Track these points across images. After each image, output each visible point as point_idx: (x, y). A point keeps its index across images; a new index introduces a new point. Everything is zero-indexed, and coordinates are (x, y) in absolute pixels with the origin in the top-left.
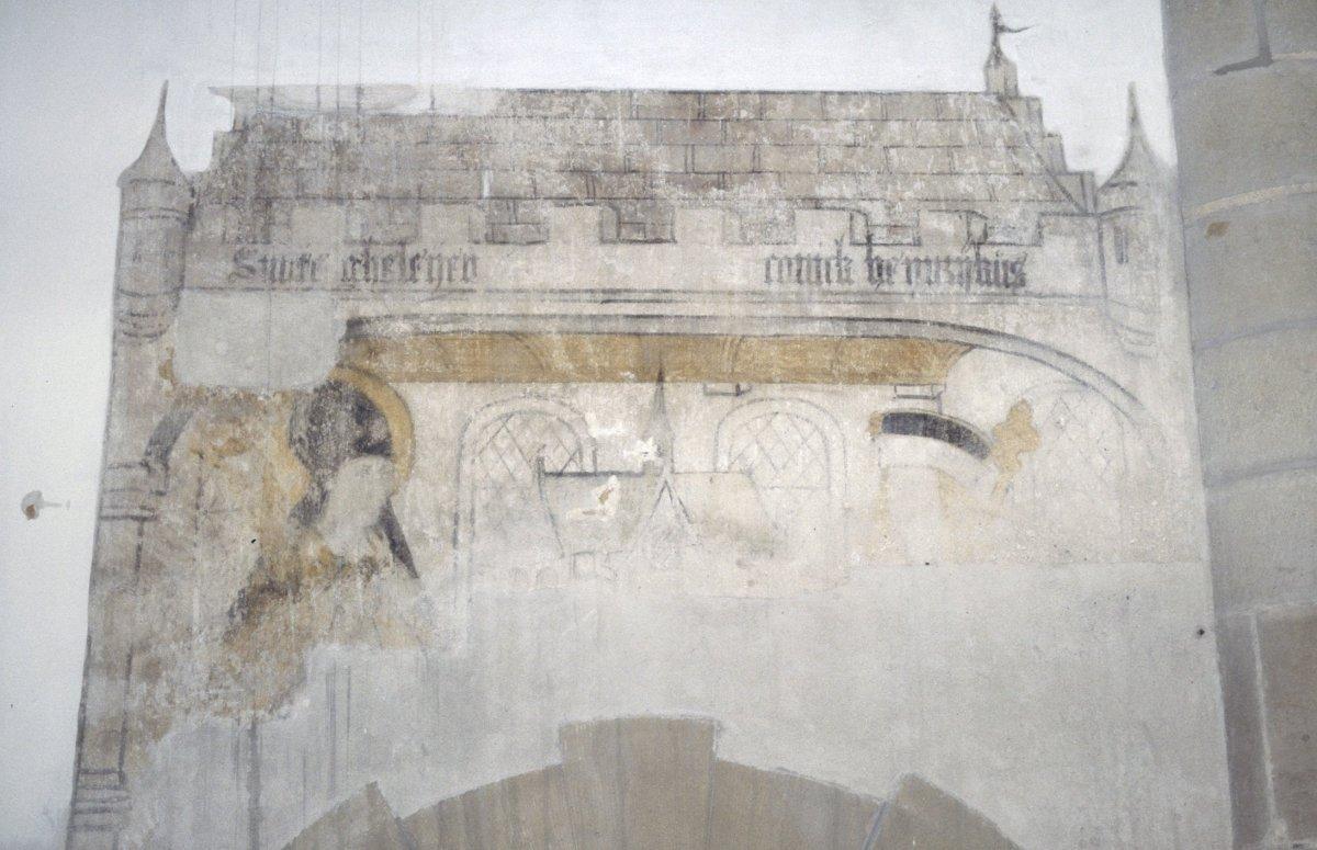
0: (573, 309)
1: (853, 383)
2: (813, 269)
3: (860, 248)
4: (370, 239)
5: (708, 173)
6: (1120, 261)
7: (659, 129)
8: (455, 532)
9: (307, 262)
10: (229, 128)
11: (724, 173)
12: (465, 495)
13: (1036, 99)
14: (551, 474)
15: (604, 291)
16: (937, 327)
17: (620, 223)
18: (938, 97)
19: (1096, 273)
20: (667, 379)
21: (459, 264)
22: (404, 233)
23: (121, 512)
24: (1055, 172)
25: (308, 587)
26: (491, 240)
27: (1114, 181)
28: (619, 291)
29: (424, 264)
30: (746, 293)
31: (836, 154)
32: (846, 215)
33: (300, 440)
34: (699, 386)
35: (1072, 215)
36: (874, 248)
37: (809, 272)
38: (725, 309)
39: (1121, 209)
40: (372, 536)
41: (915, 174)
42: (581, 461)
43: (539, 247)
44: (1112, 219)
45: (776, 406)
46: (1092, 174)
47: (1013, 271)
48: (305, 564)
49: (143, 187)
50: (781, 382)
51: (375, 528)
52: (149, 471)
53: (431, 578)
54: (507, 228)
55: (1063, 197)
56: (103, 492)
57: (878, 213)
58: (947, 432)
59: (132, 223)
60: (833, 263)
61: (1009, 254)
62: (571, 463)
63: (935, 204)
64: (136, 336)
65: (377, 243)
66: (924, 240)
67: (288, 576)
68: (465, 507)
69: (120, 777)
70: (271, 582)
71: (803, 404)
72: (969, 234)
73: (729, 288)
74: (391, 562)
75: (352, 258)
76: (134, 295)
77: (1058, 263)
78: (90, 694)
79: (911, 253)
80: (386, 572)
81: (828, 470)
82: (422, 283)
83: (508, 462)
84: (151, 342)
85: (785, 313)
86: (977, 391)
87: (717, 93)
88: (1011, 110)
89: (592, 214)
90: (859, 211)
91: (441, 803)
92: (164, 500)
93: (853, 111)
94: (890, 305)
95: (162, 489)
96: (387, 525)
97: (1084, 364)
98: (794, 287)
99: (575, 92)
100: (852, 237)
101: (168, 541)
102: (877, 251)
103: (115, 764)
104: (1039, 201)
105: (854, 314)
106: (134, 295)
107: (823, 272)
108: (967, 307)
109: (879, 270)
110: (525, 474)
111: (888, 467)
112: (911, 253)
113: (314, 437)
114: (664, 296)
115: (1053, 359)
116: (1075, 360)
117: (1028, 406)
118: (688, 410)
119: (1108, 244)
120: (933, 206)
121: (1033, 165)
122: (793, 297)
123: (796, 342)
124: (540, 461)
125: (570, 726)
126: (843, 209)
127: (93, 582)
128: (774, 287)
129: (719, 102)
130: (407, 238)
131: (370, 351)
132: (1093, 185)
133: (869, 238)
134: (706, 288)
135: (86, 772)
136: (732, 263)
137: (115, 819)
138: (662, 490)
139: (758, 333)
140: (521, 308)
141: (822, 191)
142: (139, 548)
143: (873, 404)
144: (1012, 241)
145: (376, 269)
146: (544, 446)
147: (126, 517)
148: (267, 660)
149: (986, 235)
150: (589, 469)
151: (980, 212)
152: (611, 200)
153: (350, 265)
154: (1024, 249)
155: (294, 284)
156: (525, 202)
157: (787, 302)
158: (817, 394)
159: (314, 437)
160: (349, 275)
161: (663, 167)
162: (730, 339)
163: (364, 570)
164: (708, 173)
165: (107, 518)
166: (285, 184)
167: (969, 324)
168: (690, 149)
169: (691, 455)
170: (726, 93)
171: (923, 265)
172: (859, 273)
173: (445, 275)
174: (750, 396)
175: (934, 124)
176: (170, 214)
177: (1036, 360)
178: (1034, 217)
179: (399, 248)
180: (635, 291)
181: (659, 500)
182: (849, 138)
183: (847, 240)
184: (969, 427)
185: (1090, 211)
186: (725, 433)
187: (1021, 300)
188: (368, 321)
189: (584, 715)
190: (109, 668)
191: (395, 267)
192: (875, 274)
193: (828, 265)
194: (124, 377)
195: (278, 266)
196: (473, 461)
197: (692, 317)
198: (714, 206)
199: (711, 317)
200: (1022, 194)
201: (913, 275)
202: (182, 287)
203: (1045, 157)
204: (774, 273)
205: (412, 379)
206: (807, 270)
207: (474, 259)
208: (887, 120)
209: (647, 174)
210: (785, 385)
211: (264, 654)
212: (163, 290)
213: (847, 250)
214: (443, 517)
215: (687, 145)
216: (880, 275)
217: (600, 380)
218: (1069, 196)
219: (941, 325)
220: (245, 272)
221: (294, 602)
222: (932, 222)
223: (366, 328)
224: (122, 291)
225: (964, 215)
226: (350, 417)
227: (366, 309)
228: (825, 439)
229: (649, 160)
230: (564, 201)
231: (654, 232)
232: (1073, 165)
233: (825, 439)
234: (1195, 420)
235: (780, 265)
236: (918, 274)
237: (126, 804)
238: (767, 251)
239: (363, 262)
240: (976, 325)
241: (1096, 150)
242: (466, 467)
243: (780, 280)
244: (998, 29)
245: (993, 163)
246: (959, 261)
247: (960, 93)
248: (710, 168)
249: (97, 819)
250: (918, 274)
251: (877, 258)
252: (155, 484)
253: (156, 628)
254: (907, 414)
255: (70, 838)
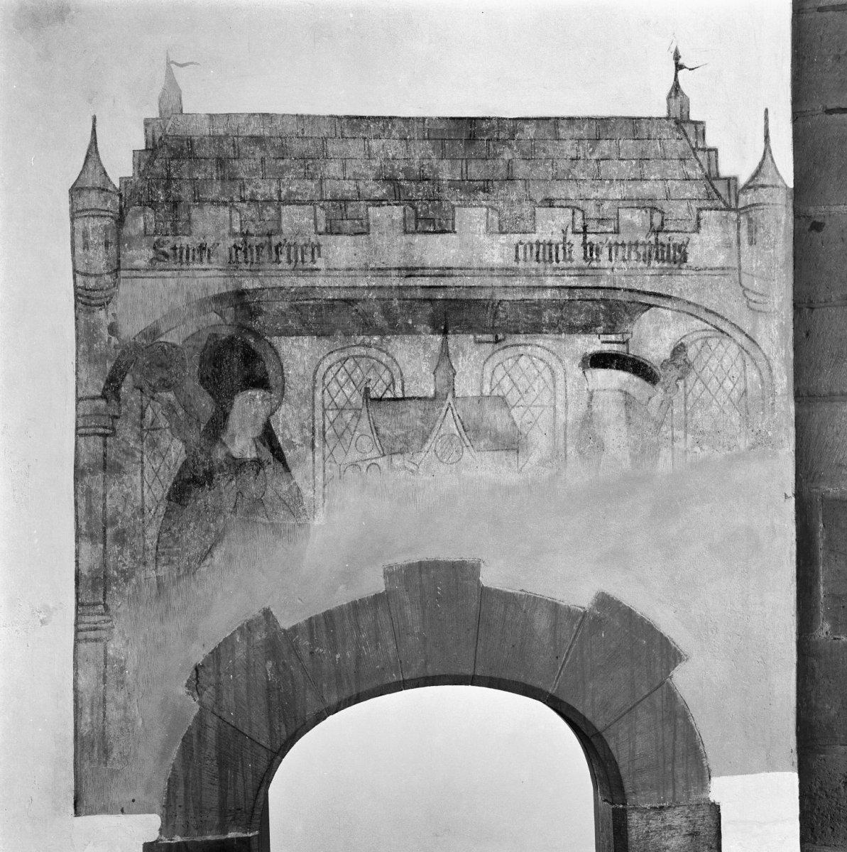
0: (387, 282)
1: (572, 333)
2: (547, 251)
3: (579, 235)
4: (247, 231)
5: (477, 181)
6: (751, 243)
7: (443, 147)
8: (313, 441)
9: (204, 249)
10: (144, 148)
11: (488, 180)
12: (318, 413)
13: (702, 123)
14: (375, 399)
15: (407, 269)
16: (627, 292)
17: (417, 219)
18: (634, 122)
19: (735, 255)
20: (450, 332)
21: (309, 250)
22: (270, 226)
23: (91, 430)
24: (711, 177)
25: (218, 479)
26: (329, 231)
27: (751, 184)
28: (417, 269)
29: (285, 250)
30: (503, 269)
31: (563, 165)
32: (570, 211)
33: (208, 378)
34: (471, 337)
35: (722, 210)
36: (588, 235)
37: (544, 253)
38: (487, 281)
39: (754, 205)
40: (259, 444)
41: (617, 180)
42: (394, 389)
43: (364, 237)
44: (747, 212)
45: (521, 349)
46: (735, 179)
47: (680, 252)
48: (215, 464)
49: (85, 193)
50: (524, 333)
51: (260, 438)
52: (107, 402)
53: (298, 474)
54: (339, 223)
55: (716, 197)
56: (78, 416)
57: (592, 212)
58: (631, 366)
59: (80, 221)
60: (561, 246)
61: (678, 239)
62: (388, 392)
63: (630, 202)
64: (90, 305)
65: (252, 235)
66: (622, 229)
67: (205, 471)
68: (319, 423)
69: (104, 607)
70: (194, 477)
71: (539, 349)
72: (652, 224)
73: (491, 266)
74: (272, 462)
75: (235, 246)
76: (86, 274)
77: (708, 245)
78: (80, 554)
79: (612, 238)
80: (269, 470)
81: (555, 393)
82: (284, 264)
83: (346, 391)
84: (101, 309)
85: (527, 284)
86: (654, 337)
87: (483, 119)
88: (684, 131)
89: (397, 212)
90: (578, 209)
91: (311, 618)
92: (119, 422)
93: (577, 133)
94: (598, 281)
95: (117, 414)
96: (268, 437)
97: (722, 318)
98: (535, 264)
99: (384, 118)
100: (573, 227)
101: (123, 450)
102: (590, 237)
103: (101, 600)
104: (699, 199)
105: (573, 284)
106: (86, 274)
107: (554, 253)
108: (648, 278)
109: (590, 250)
110: (357, 399)
111: (593, 391)
112: (612, 238)
113: (216, 375)
114: (447, 272)
115: (703, 315)
116: (717, 315)
117: (684, 347)
118: (464, 355)
119: (744, 232)
120: (628, 204)
121: (696, 173)
122: (534, 272)
123: (534, 304)
124: (367, 390)
125: (390, 567)
126: (568, 207)
127: (76, 479)
128: (521, 265)
129: (484, 125)
130: (272, 230)
131: (251, 314)
132: (736, 187)
133: (585, 228)
134: (475, 266)
135: (82, 605)
136: (493, 248)
137: (104, 634)
138: (447, 410)
139: (510, 299)
140: (348, 282)
141: (558, 192)
142: (105, 455)
143: (584, 347)
144: (679, 229)
145: (252, 254)
146: (370, 380)
147: (95, 434)
148: (195, 528)
149: (662, 224)
150: (400, 396)
151: (659, 208)
152: (411, 202)
153: (234, 250)
154: (687, 235)
155: (196, 266)
156: (352, 203)
157: (529, 276)
158: (546, 341)
159: (216, 375)
160: (234, 259)
161: (445, 176)
162: (491, 302)
163: (255, 467)
164: (477, 181)
165: (81, 435)
166: (186, 193)
167: (649, 290)
168: (464, 161)
169: (466, 386)
170: (490, 119)
171: (620, 248)
172: (578, 252)
173: (300, 258)
174: (504, 344)
175: (632, 141)
176: (107, 213)
177: (692, 315)
178: (695, 210)
179: (266, 239)
180: (428, 268)
181: (445, 416)
182: (573, 154)
183: (570, 230)
184: (648, 364)
185: (733, 207)
186: (488, 369)
187: (683, 272)
188: (249, 293)
189: (402, 560)
190: (92, 536)
191: (265, 252)
192: (588, 255)
193: (557, 248)
194: (86, 335)
195: (185, 252)
196: (323, 392)
197: (466, 287)
198: (481, 206)
199: (479, 287)
200: (688, 195)
201: (613, 254)
202: (118, 269)
203: (705, 166)
204: (521, 255)
205: (280, 335)
206: (546, 252)
207: (319, 246)
208: (599, 139)
209: (435, 181)
210: (528, 335)
211: (192, 525)
212: (106, 271)
213: (570, 237)
214: (304, 430)
215: (463, 159)
216: (591, 255)
217: (406, 333)
218: (719, 195)
219: (631, 291)
220: (162, 257)
221: (210, 489)
222: (626, 216)
223: (247, 298)
224: (78, 272)
225: (649, 210)
226: (236, 362)
227: (249, 284)
228: (553, 373)
229: (436, 172)
230: (378, 202)
231: (440, 224)
232: (725, 170)
233: (553, 373)
234: (792, 355)
235: (525, 249)
236: (616, 254)
237: (110, 624)
238: (516, 238)
239: (243, 249)
240: (653, 291)
241: (736, 163)
242: (318, 395)
243: (525, 260)
244: (679, 67)
245: (669, 172)
246: (644, 244)
247: (650, 118)
248: (478, 177)
249: (92, 634)
250: (616, 254)
251: (590, 243)
252: (113, 411)
253: (120, 509)
254: (606, 354)
255: (75, 646)
